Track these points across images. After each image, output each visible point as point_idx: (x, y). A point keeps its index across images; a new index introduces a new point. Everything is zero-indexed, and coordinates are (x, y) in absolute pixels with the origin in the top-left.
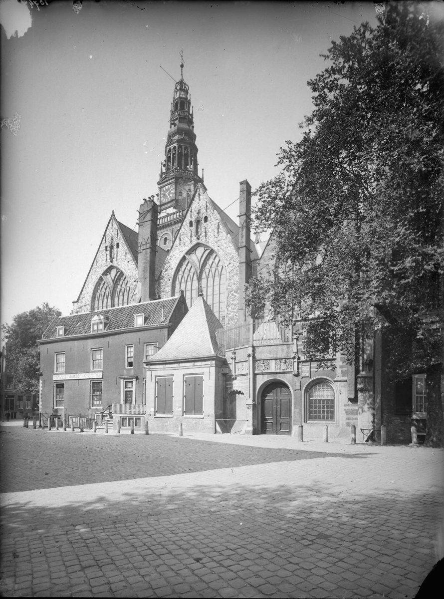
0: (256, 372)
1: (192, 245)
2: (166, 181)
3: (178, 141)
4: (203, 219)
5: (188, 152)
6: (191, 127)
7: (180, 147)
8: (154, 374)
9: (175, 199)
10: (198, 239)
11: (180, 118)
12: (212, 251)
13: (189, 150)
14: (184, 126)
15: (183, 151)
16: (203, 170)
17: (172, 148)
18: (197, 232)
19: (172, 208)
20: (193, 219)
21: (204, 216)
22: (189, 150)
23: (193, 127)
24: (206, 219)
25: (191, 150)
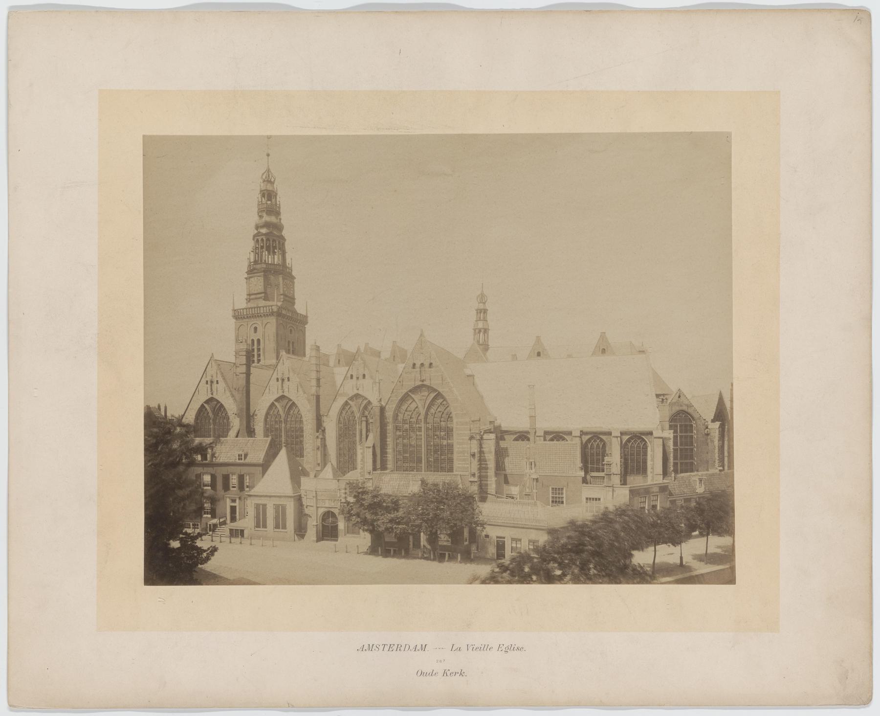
0: (318, 506)
1: (279, 396)
2: (254, 273)
3: (265, 235)
4: (287, 379)
5: (276, 244)
6: (278, 220)
7: (268, 240)
8: (254, 502)
9: (265, 293)
10: (283, 392)
11: (267, 210)
12: (294, 403)
13: (277, 242)
14: (273, 219)
15: (271, 244)
16: (291, 259)
17: (260, 239)
18: (282, 387)
19: (261, 300)
20: (279, 377)
21: (287, 377)
22: (277, 242)
23: (280, 219)
24: (288, 378)
25: (279, 242)
